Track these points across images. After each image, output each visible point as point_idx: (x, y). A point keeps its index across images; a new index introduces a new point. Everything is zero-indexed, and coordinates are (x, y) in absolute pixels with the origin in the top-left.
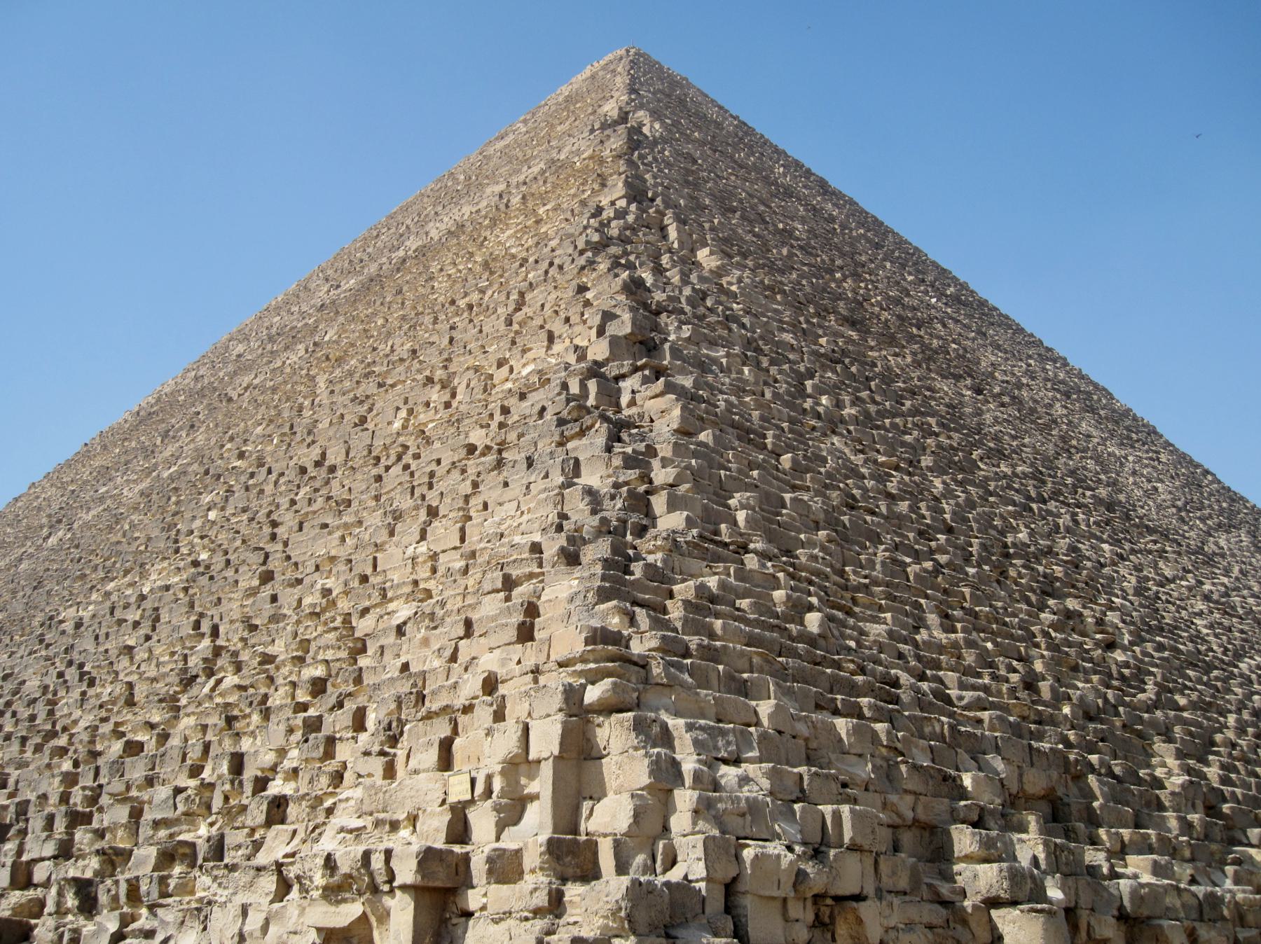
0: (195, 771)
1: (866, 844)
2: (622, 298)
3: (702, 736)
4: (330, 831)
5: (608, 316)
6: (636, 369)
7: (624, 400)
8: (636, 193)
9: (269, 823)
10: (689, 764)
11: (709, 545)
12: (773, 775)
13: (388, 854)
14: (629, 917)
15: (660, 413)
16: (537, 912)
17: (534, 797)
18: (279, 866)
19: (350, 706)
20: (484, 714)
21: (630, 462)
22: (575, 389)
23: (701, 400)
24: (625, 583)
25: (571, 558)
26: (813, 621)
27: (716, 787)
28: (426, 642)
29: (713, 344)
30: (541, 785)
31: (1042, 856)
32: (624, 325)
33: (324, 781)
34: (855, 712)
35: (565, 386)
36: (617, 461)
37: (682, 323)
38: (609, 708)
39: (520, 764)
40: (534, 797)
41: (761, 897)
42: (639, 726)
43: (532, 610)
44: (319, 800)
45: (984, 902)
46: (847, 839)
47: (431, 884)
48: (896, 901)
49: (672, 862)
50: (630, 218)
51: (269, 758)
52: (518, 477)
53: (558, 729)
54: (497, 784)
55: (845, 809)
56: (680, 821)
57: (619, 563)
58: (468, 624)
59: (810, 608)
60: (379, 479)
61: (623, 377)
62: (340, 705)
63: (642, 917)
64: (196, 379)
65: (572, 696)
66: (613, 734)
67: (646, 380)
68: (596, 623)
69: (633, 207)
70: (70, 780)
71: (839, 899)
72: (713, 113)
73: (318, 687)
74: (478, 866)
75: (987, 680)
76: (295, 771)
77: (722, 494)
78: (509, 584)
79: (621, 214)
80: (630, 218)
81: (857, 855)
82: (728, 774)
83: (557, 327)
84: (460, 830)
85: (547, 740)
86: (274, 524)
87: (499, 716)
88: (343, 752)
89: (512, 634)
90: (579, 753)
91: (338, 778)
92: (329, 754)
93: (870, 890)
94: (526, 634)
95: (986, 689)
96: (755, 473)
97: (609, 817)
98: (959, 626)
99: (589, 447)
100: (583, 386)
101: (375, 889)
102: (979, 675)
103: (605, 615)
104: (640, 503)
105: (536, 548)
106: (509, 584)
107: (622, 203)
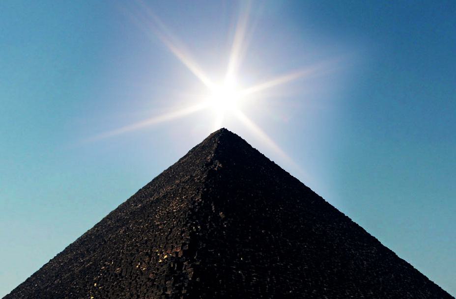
5: (184, 244)
15: (190, 272)
32: (186, 248)
35: (170, 265)
52: (155, 290)
64: (98, 231)
67: (189, 263)
69: (203, 202)
86: (108, 292)
100: (174, 265)
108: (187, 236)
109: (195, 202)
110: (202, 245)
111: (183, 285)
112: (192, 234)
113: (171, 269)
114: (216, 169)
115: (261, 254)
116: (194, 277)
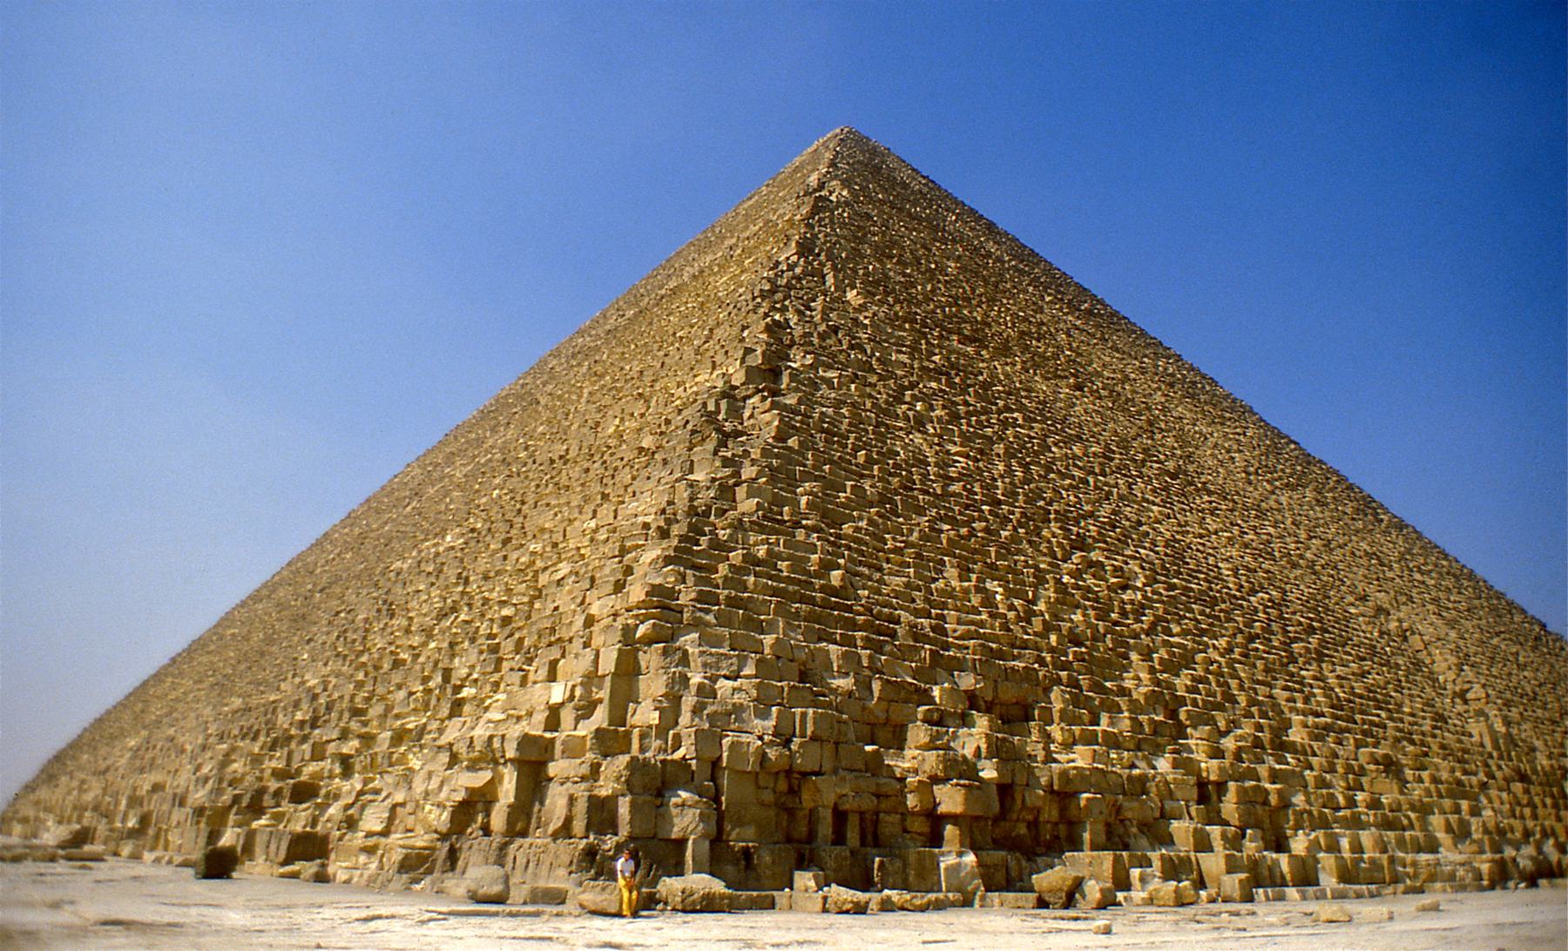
0: (425, 680)
1: (825, 736)
2: (764, 336)
3: (710, 660)
4: (482, 721)
6: (758, 391)
7: (747, 414)
8: (805, 249)
9: (450, 717)
10: (696, 679)
11: (769, 521)
12: (758, 687)
13: (503, 736)
14: (627, 781)
16: (583, 779)
17: (600, 701)
18: (451, 745)
19: (517, 636)
20: (577, 645)
21: (726, 462)
22: (711, 407)
23: (798, 413)
24: (691, 552)
25: (664, 534)
26: (836, 576)
27: (713, 694)
28: (570, 592)
29: (829, 367)
30: (604, 694)
31: (984, 746)
32: (757, 359)
33: (488, 688)
34: (848, 641)
35: (705, 405)
36: (718, 464)
37: (807, 353)
38: (649, 641)
39: (592, 678)
40: (600, 701)
41: (738, 772)
42: (665, 653)
43: (629, 571)
44: (483, 701)
45: (930, 777)
46: (809, 733)
47: (527, 758)
48: (849, 776)
49: (677, 747)
50: (798, 270)
51: (464, 671)
53: (615, 655)
54: (578, 692)
55: (811, 711)
56: (685, 718)
57: (689, 539)
58: (593, 579)
59: (838, 567)
60: (587, 470)
61: (749, 397)
62: (511, 635)
63: (637, 781)
65: (628, 631)
66: (650, 658)
67: (764, 399)
68: (658, 581)
70: (360, 685)
71: (805, 775)
72: (904, 175)
73: (506, 621)
74: (558, 747)
75: (984, 617)
76: (476, 681)
77: (792, 483)
78: (623, 551)
79: (791, 267)
80: (798, 270)
81: (817, 744)
82: (724, 686)
83: (719, 358)
84: (553, 723)
85: (608, 664)
87: (586, 645)
88: (506, 665)
89: (610, 588)
90: (628, 671)
91: (496, 685)
92: (497, 669)
93: (827, 767)
94: (619, 587)
95: (982, 624)
96: (827, 467)
97: (645, 714)
98: (974, 577)
99: (703, 451)
100: (717, 405)
101: (496, 763)
102: (979, 613)
103: (666, 576)
104: (726, 492)
105: (646, 526)
106: (623, 551)
107: (795, 258)
108: (757, 336)
109: (778, 263)
110: (799, 360)
111: (746, 453)
112: (774, 329)
113: (711, 418)
114: (833, 198)
115: (971, 400)
116: (781, 437)
